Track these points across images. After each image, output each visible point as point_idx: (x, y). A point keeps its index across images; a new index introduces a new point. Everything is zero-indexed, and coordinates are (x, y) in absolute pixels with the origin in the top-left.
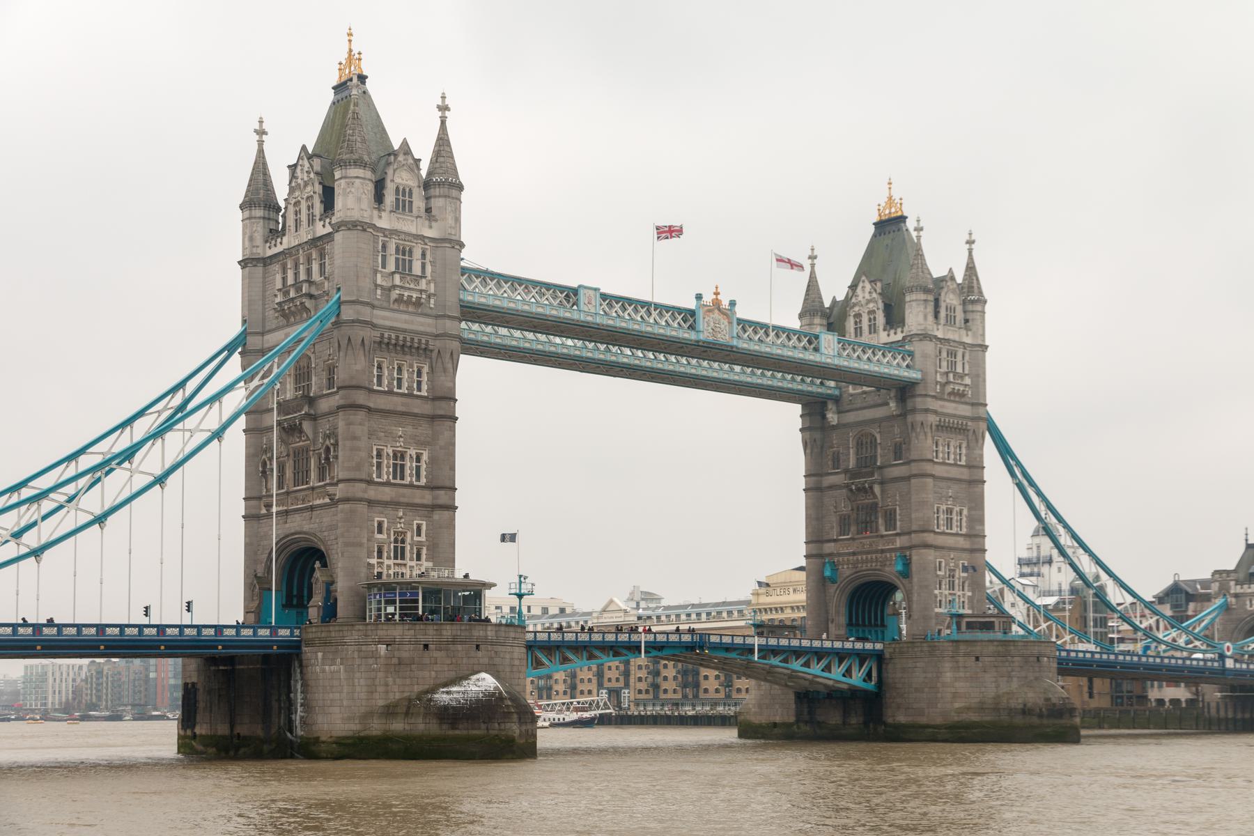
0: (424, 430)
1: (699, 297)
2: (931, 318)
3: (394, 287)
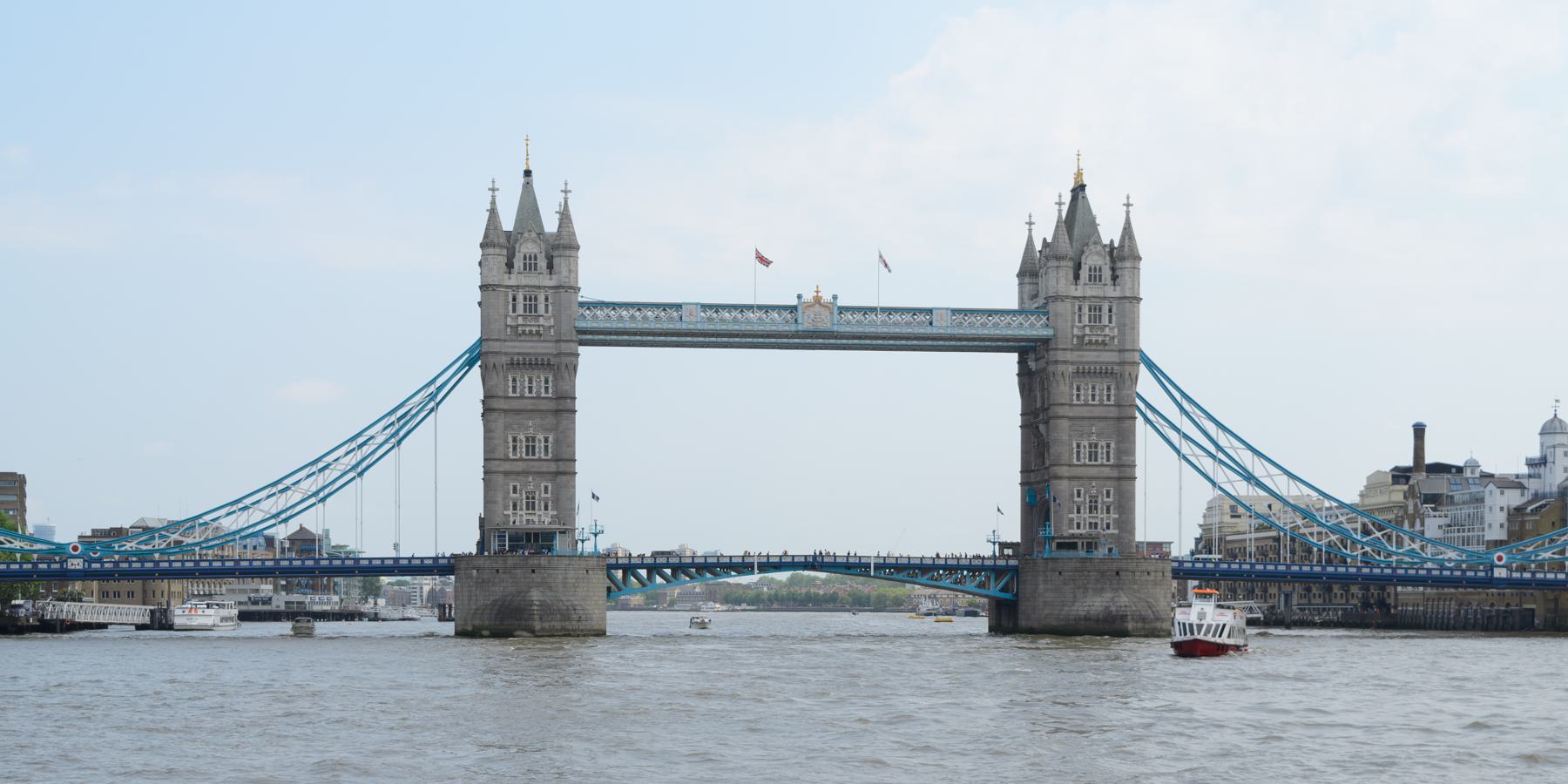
0: (550, 420)
1: (799, 297)
2: (1063, 282)
3: (517, 326)
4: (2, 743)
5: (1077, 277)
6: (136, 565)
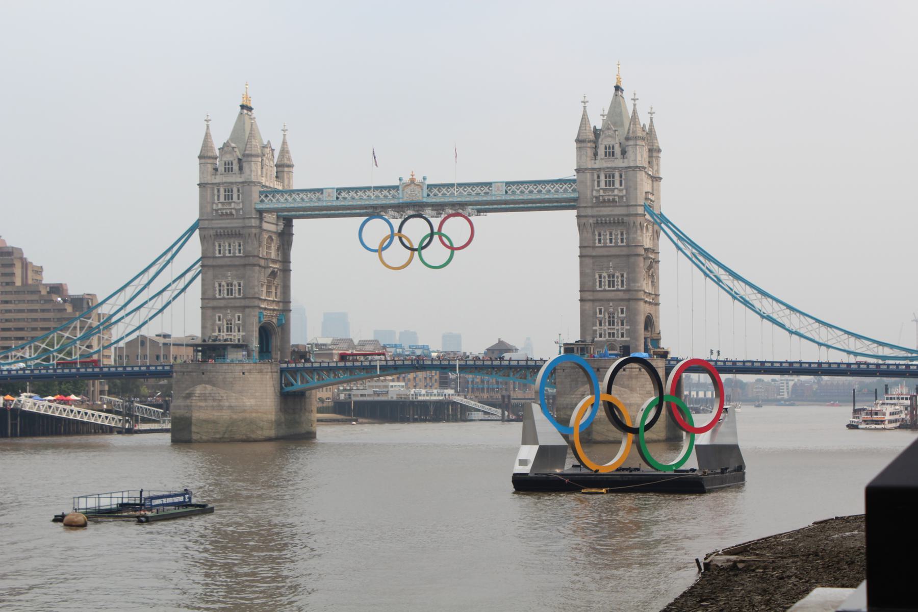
3: (219, 209)
4: (2, 486)
5: (596, 155)
6: (44, 372)
